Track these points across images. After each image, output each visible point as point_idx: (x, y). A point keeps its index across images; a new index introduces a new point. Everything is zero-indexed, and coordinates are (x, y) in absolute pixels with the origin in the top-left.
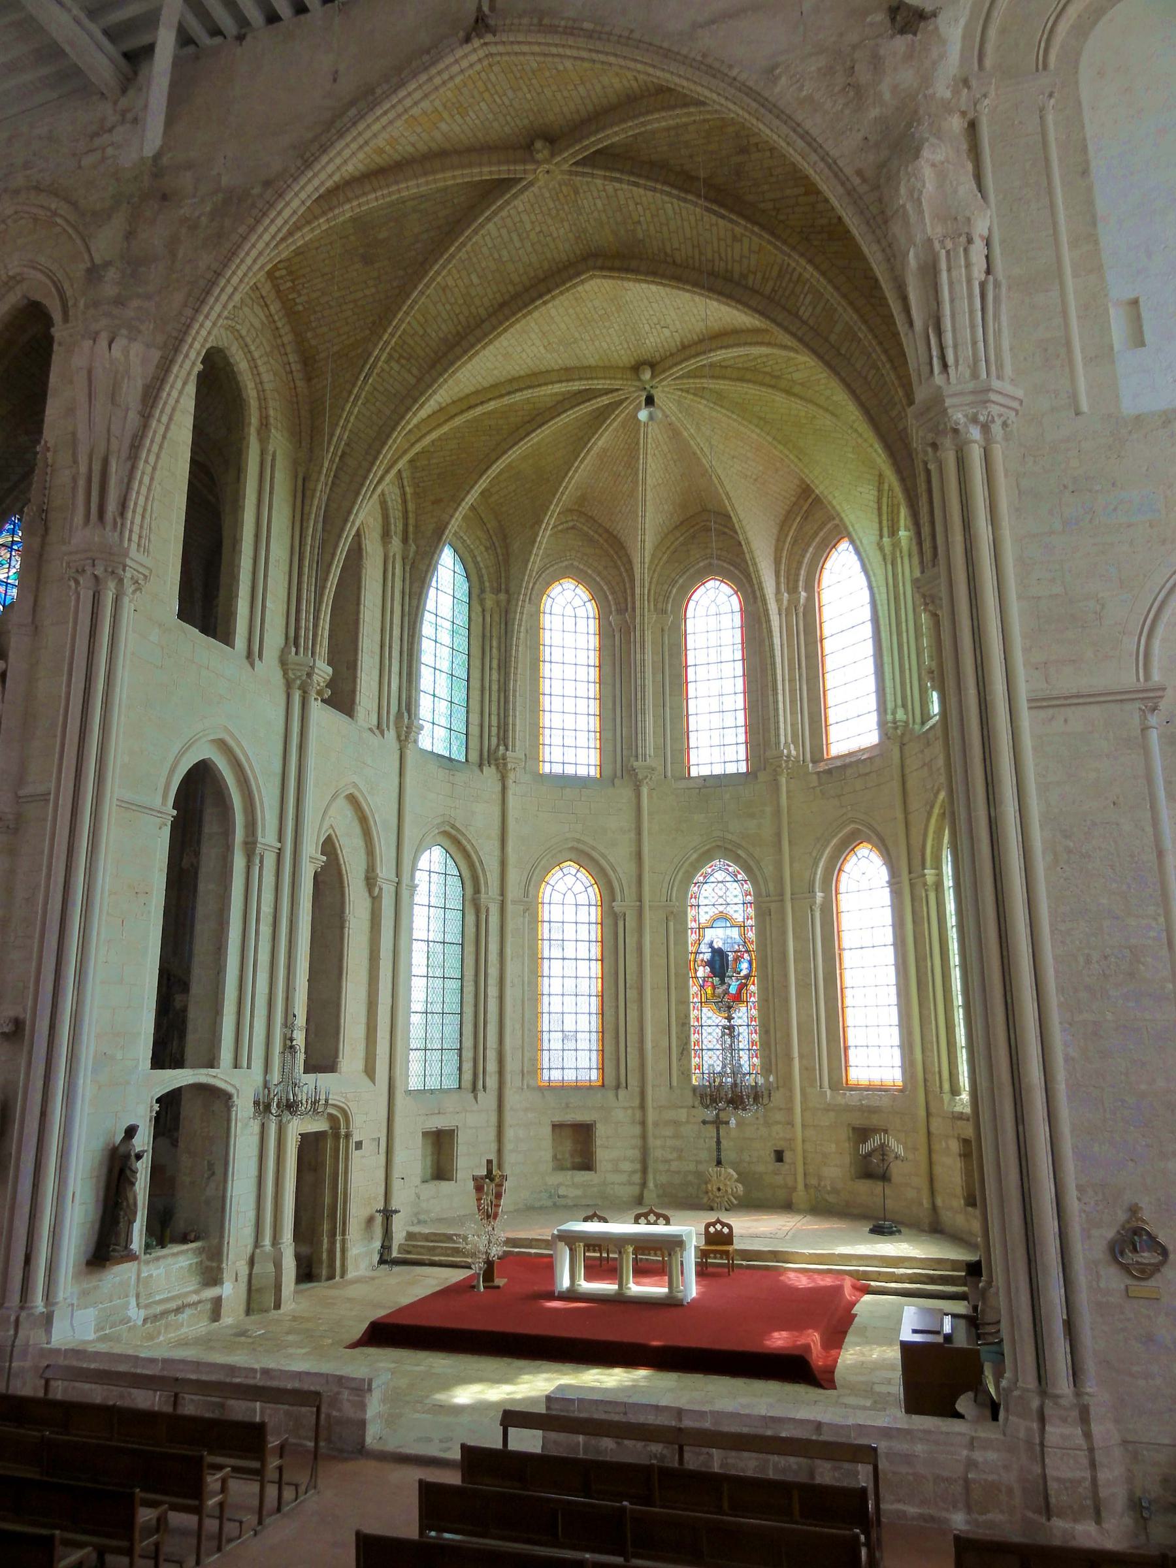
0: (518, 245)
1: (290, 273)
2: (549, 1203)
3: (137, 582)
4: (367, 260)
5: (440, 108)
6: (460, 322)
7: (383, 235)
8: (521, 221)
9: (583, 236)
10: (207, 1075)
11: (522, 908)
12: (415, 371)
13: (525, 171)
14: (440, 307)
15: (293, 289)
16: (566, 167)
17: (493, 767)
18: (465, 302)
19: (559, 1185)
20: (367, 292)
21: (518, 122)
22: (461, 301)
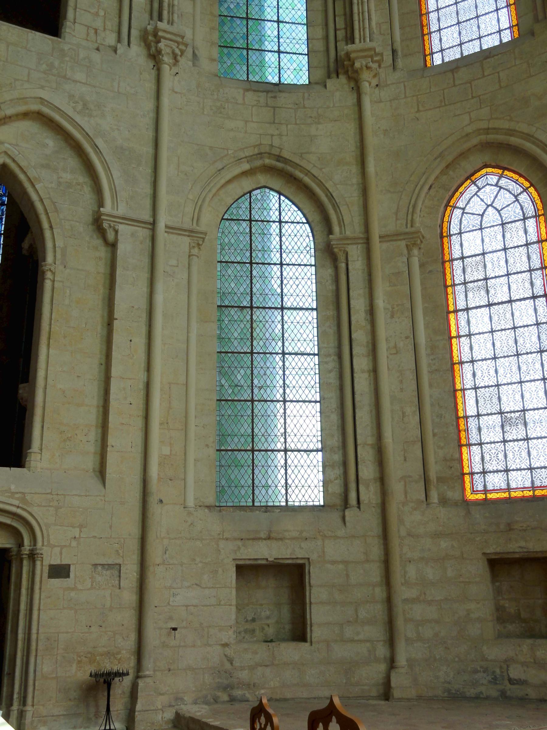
2: (494, 693)
11: (403, 244)
17: (343, 79)
19: (508, 662)
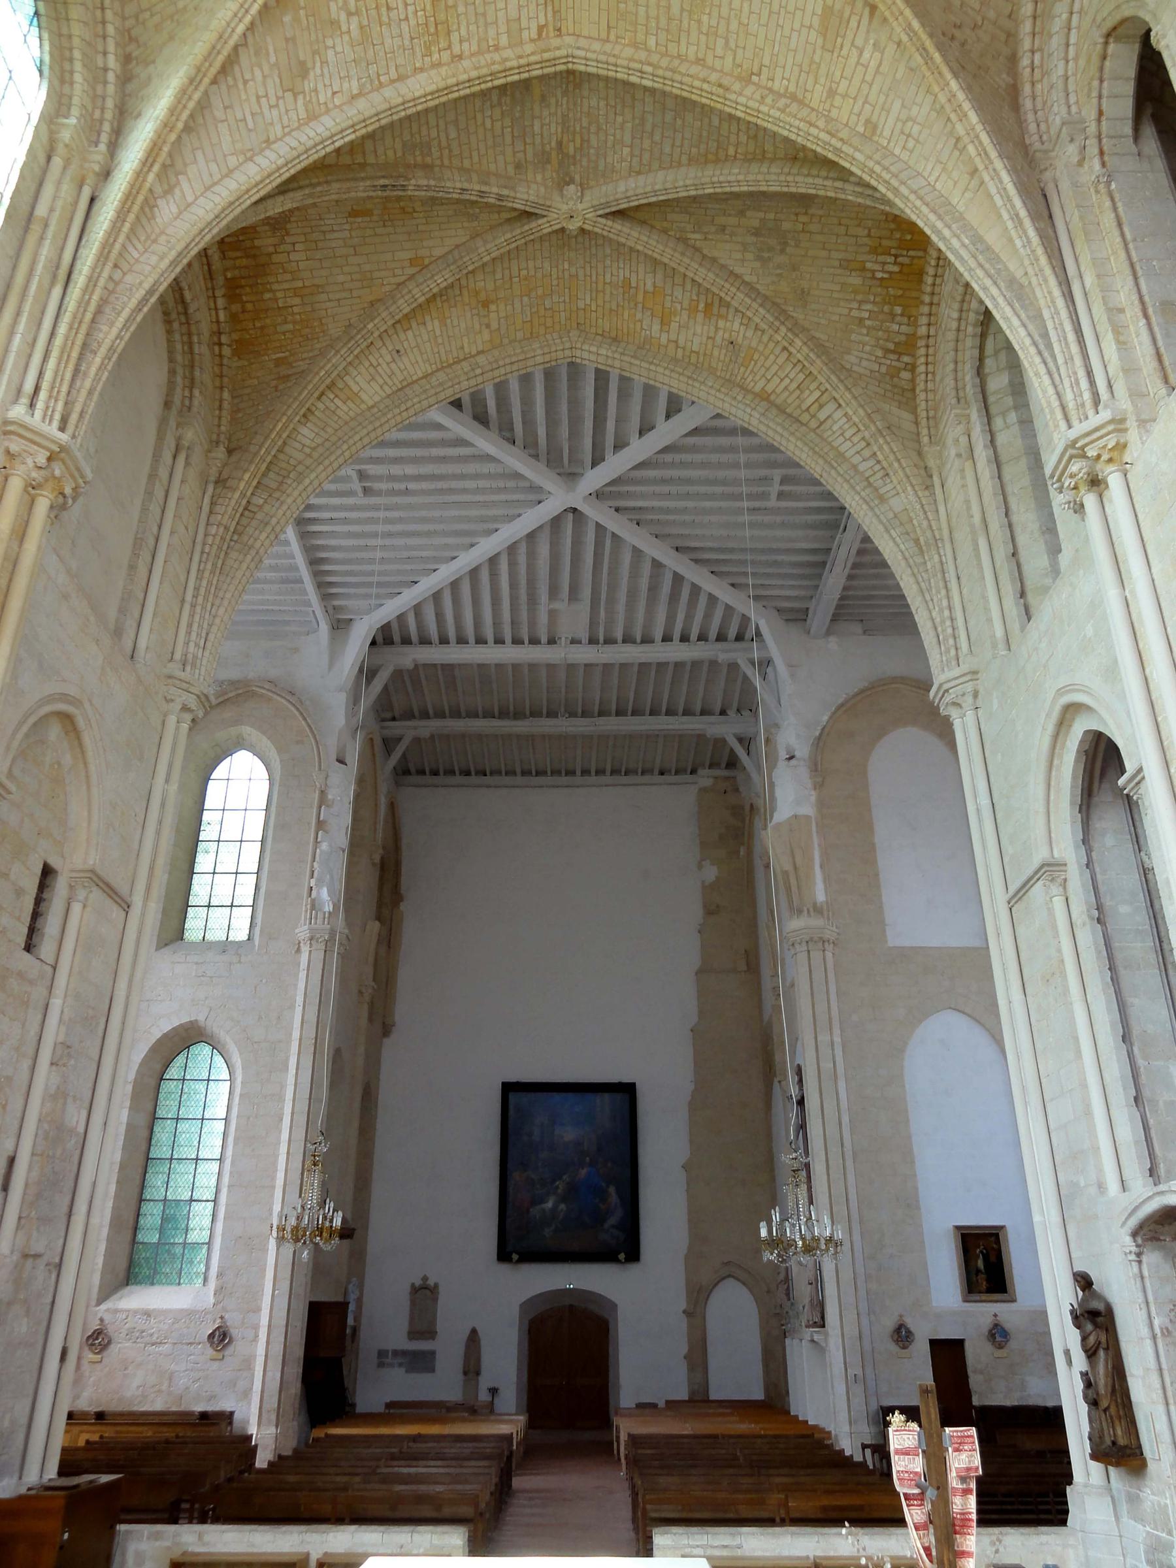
0: (650, 118)
8: (633, 138)
9: (571, 88)
21: (587, 243)
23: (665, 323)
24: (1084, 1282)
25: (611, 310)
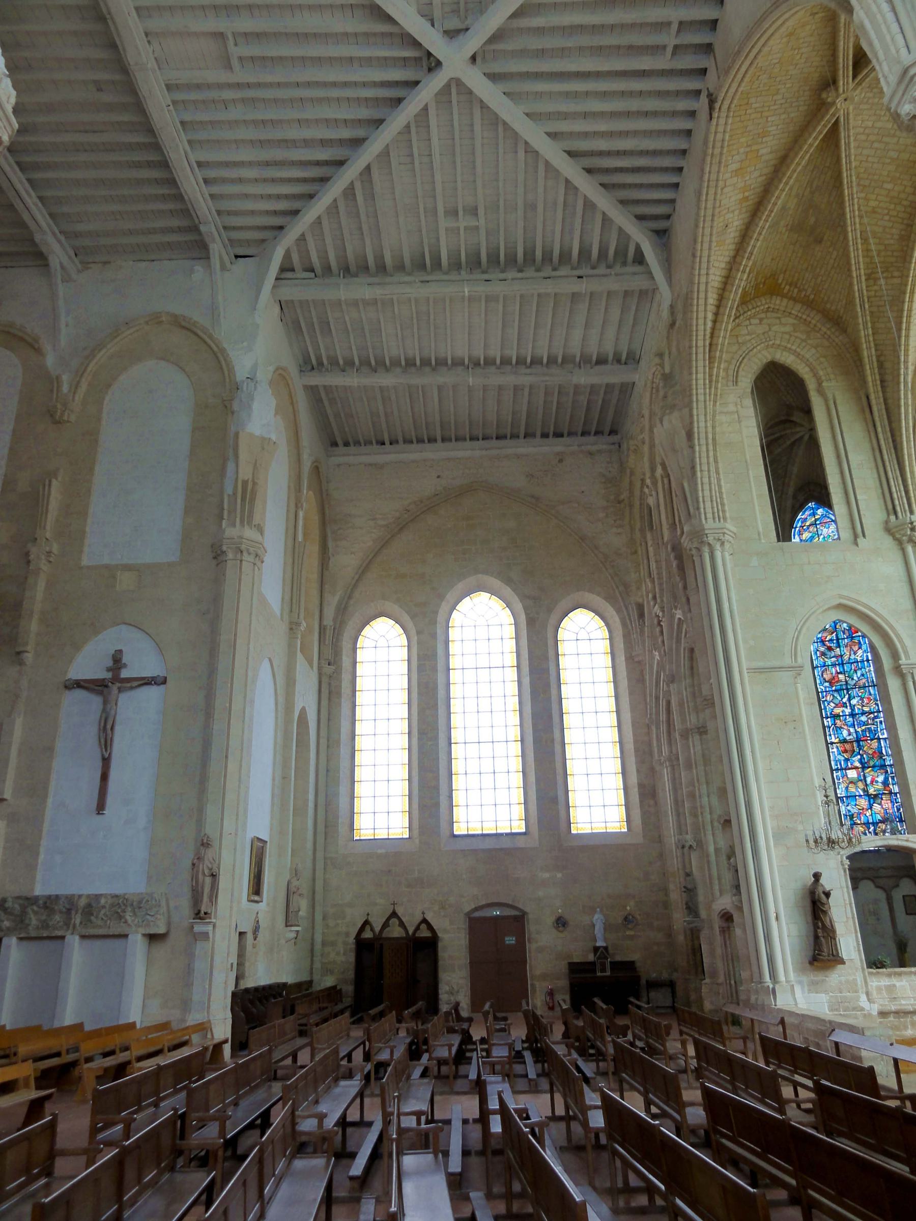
0: (895, 140)
1: (790, 285)
3: (719, 540)
4: (819, 241)
5: (748, 149)
6: (903, 219)
7: (812, 220)
10: (897, 839)
12: (896, 274)
13: (833, 115)
14: (880, 223)
15: (800, 291)
16: (851, 86)
18: (896, 204)
20: (834, 256)
22: (892, 206)
23: (736, 173)
24: (817, 876)
25: (746, 127)
